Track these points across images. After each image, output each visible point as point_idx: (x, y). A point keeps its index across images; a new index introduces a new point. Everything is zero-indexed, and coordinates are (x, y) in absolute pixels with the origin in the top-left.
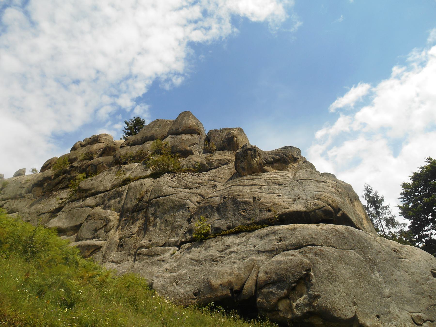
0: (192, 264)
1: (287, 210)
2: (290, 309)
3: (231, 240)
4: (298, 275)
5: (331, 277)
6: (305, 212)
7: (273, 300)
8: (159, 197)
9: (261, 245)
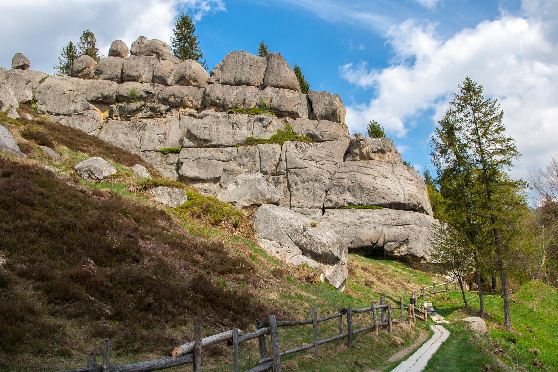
0: (342, 225)
1: (395, 201)
2: (399, 252)
5: (417, 239)
6: (404, 204)
7: (393, 248)
8: (296, 168)
9: (383, 219)
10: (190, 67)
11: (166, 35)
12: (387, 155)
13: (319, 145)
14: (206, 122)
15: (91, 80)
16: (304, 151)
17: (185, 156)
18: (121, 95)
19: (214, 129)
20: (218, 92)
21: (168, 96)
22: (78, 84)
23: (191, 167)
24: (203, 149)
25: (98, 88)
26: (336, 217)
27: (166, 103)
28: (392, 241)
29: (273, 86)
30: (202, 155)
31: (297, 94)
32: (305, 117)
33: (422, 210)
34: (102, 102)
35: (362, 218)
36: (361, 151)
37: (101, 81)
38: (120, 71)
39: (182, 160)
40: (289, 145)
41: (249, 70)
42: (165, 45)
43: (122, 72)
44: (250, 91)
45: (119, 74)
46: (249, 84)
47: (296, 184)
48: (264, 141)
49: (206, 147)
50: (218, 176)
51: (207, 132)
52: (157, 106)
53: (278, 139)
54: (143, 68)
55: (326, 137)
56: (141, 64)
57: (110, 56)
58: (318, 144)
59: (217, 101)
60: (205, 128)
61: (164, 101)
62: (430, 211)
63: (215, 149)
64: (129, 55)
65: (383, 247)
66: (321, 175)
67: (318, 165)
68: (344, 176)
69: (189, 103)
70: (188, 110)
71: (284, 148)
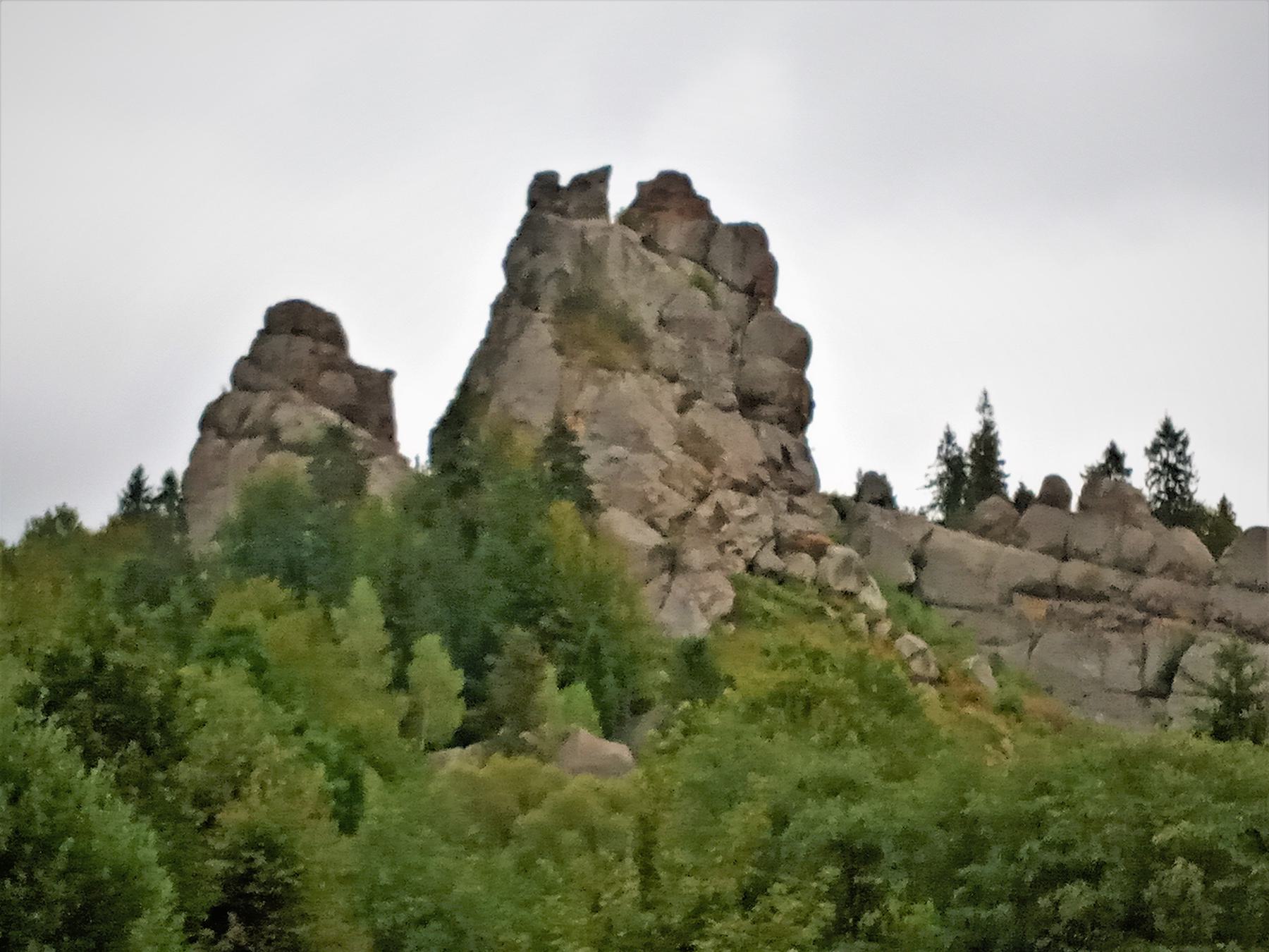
15: (1011, 549)
34: (1036, 591)
43: (1066, 539)
59: (1228, 618)
61: (1141, 606)
64: (1074, 506)
70: (1175, 623)
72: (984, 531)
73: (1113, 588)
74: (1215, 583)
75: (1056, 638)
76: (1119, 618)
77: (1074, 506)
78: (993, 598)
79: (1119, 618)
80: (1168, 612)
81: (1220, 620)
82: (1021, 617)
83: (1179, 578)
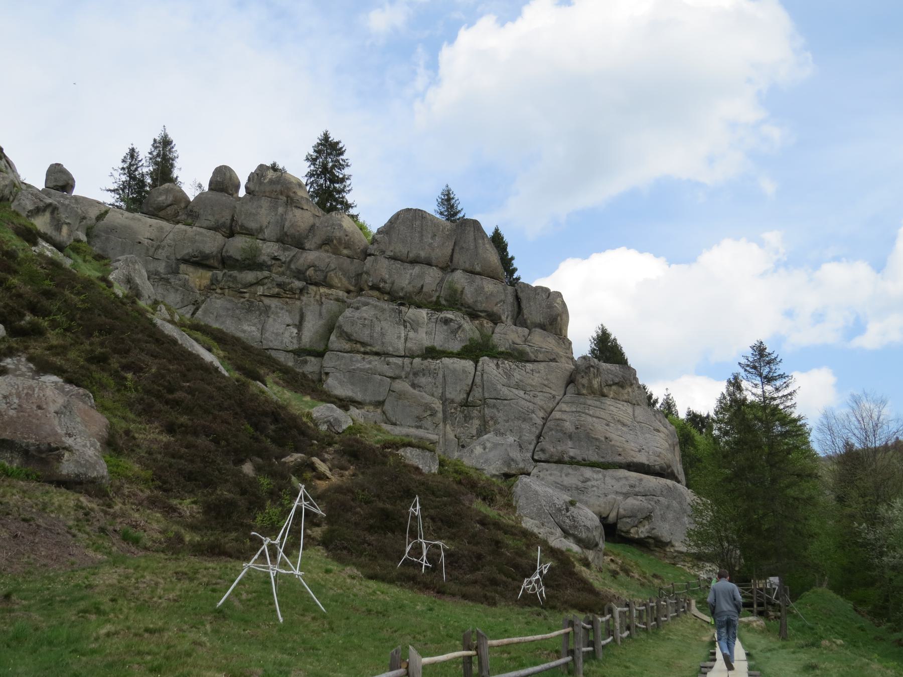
1: (635, 460)
2: (637, 532)
3: (588, 472)
4: (644, 515)
5: (663, 518)
9: (618, 486)
10: (341, 226)
11: (298, 169)
12: (626, 391)
13: (529, 366)
14: (365, 315)
15: (180, 226)
16: (509, 375)
17: (332, 364)
18: (230, 257)
19: (378, 329)
20: (382, 269)
21: (306, 267)
22: (161, 229)
23: (341, 383)
24: (359, 357)
25: (193, 241)
26: (551, 475)
27: (301, 276)
28: (629, 517)
29: (465, 271)
30: (359, 365)
31: (500, 287)
32: (509, 322)
33: (672, 476)
34: (200, 261)
35: (588, 480)
36: (590, 382)
37: (198, 229)
38: (229, 217)
39: (327, 370)
40: (487, 363)
41: (431, 241)
42: (300, 184)
43: (233, 220)
44: (432, 274)
45: (229, 222)
46: (429, 264)
47: (496, 422)
48: (450, 355)
49: (365, 353)
50: (381, 399)
51: (367, 332)
52: (287, 281)
53: (474, 351)
54: (264, 215)
55: (541, 357)
56: (263, 211)
57: (210, 189)
58: (527, 364)
59: (382, 285)
60: (364, 325)
61: (299, 274)
62: (682, 477)
63: (377, 358)
64: (242, 193)
65: (615, 524)
66: (533, 412)
67: (527, 397)
68: (564, 417)
69: (336, 280)
70: (333, 291)
71: (479, 368)
72: (156, 212)
73: (275, 258)
74: (370, 255)
75: (218, 303)
76: (279, 285)
77: (242, 193)
78: (161, 268)
79: (279, 285)
80: (325, 283)
81: (374, 287)
82: (185, 285)
83: (336, 252)
